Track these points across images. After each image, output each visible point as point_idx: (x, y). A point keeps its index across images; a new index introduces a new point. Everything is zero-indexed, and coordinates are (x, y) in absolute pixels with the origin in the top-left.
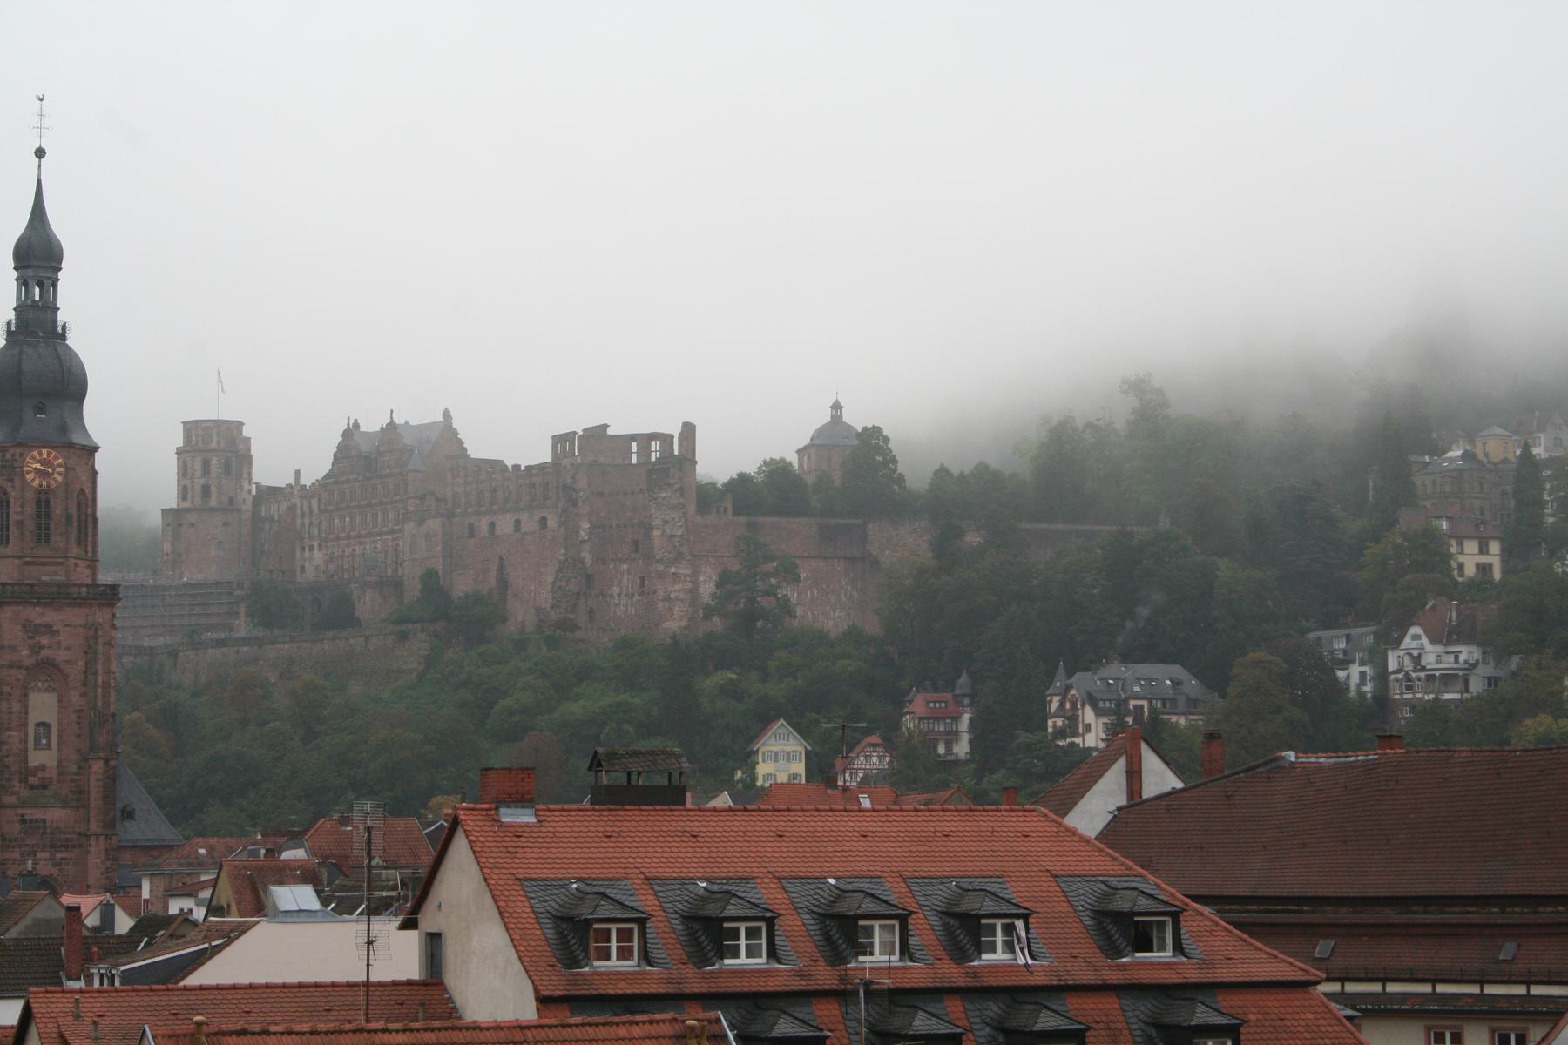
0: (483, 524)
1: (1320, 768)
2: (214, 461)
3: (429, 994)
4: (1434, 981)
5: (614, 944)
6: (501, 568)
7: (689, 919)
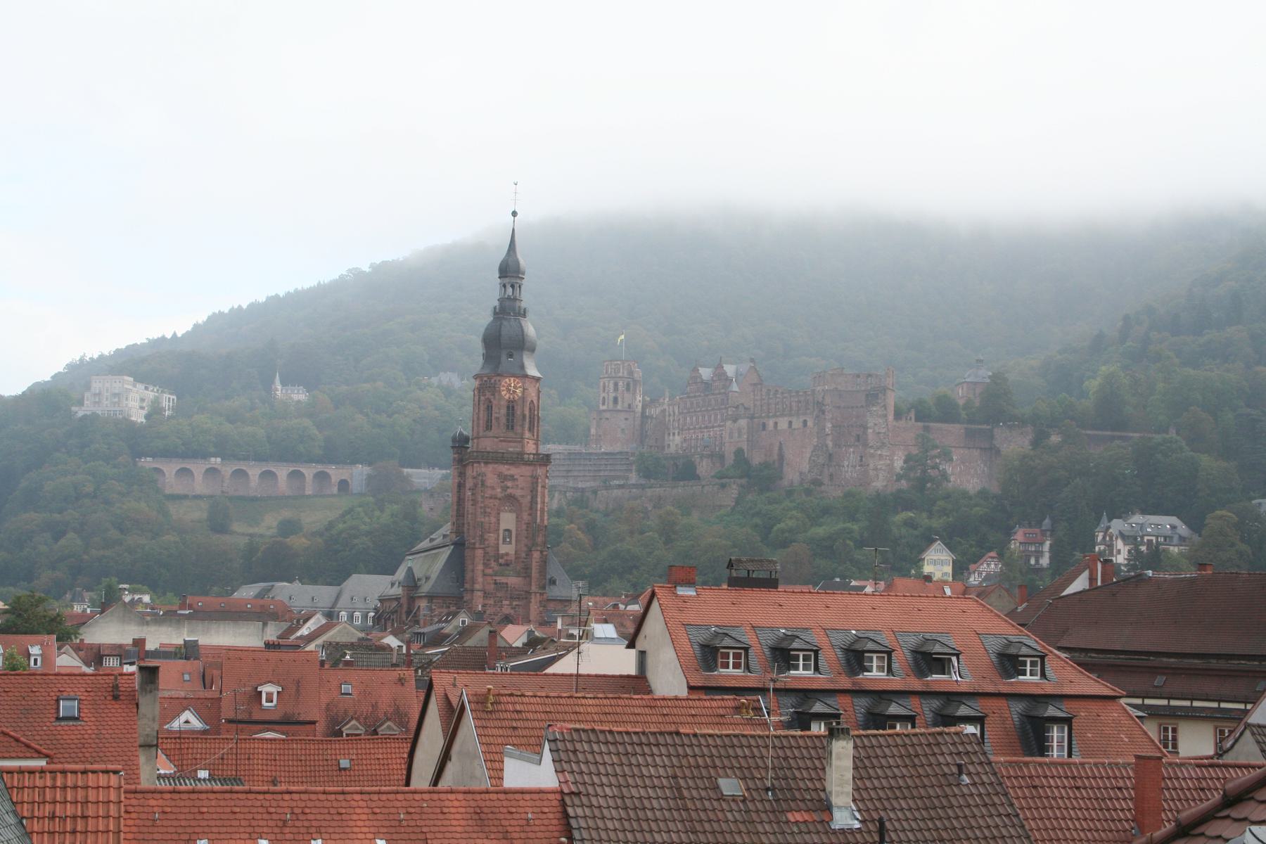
0: (771, 423)
1: (1165, 580)
2: (621, 383)
3: (638, 682)
4: (1219, 701)
5: (731, 661)
6: (780, 449)
7: (774, 649)
